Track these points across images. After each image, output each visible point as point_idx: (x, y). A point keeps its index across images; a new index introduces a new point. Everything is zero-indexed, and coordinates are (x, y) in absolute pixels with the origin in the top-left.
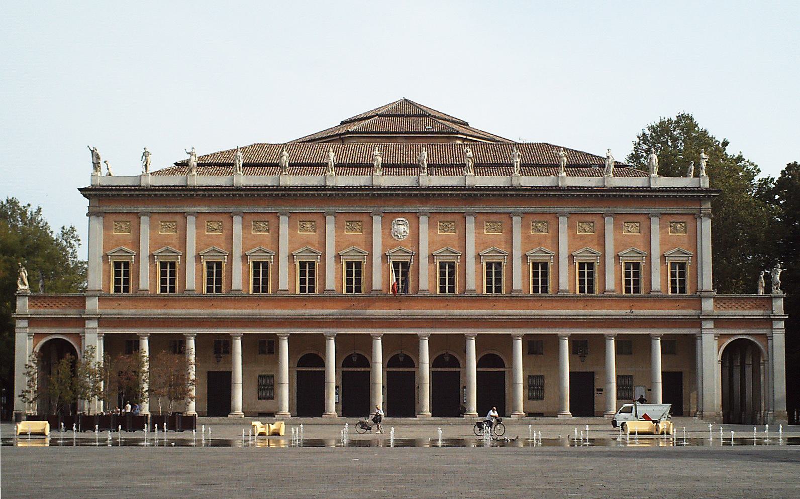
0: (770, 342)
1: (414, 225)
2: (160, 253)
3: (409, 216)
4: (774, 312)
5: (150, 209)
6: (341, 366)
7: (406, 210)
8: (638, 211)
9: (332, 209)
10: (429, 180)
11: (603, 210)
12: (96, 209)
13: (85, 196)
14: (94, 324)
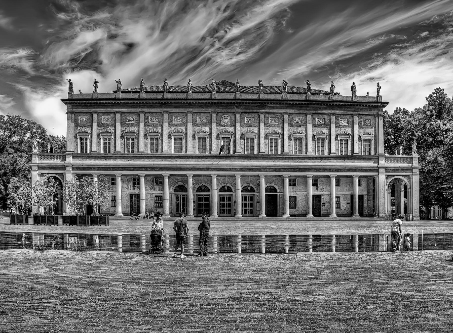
0: (411, 179)
1: (233, 119)
2: (103, 132)
3: (230, 114)
4: (414, 164)
7: (229, 110)
8: (348, 113)
9: (190, 110)
10: (241, 96)
12: (70, 110)
13: (65, 103)
14: (70, 168)
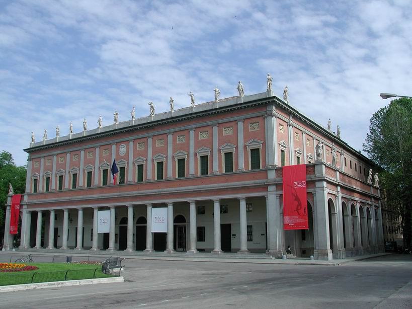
5: (56, 153)
6: (119, 223)
11: (212, 123)
